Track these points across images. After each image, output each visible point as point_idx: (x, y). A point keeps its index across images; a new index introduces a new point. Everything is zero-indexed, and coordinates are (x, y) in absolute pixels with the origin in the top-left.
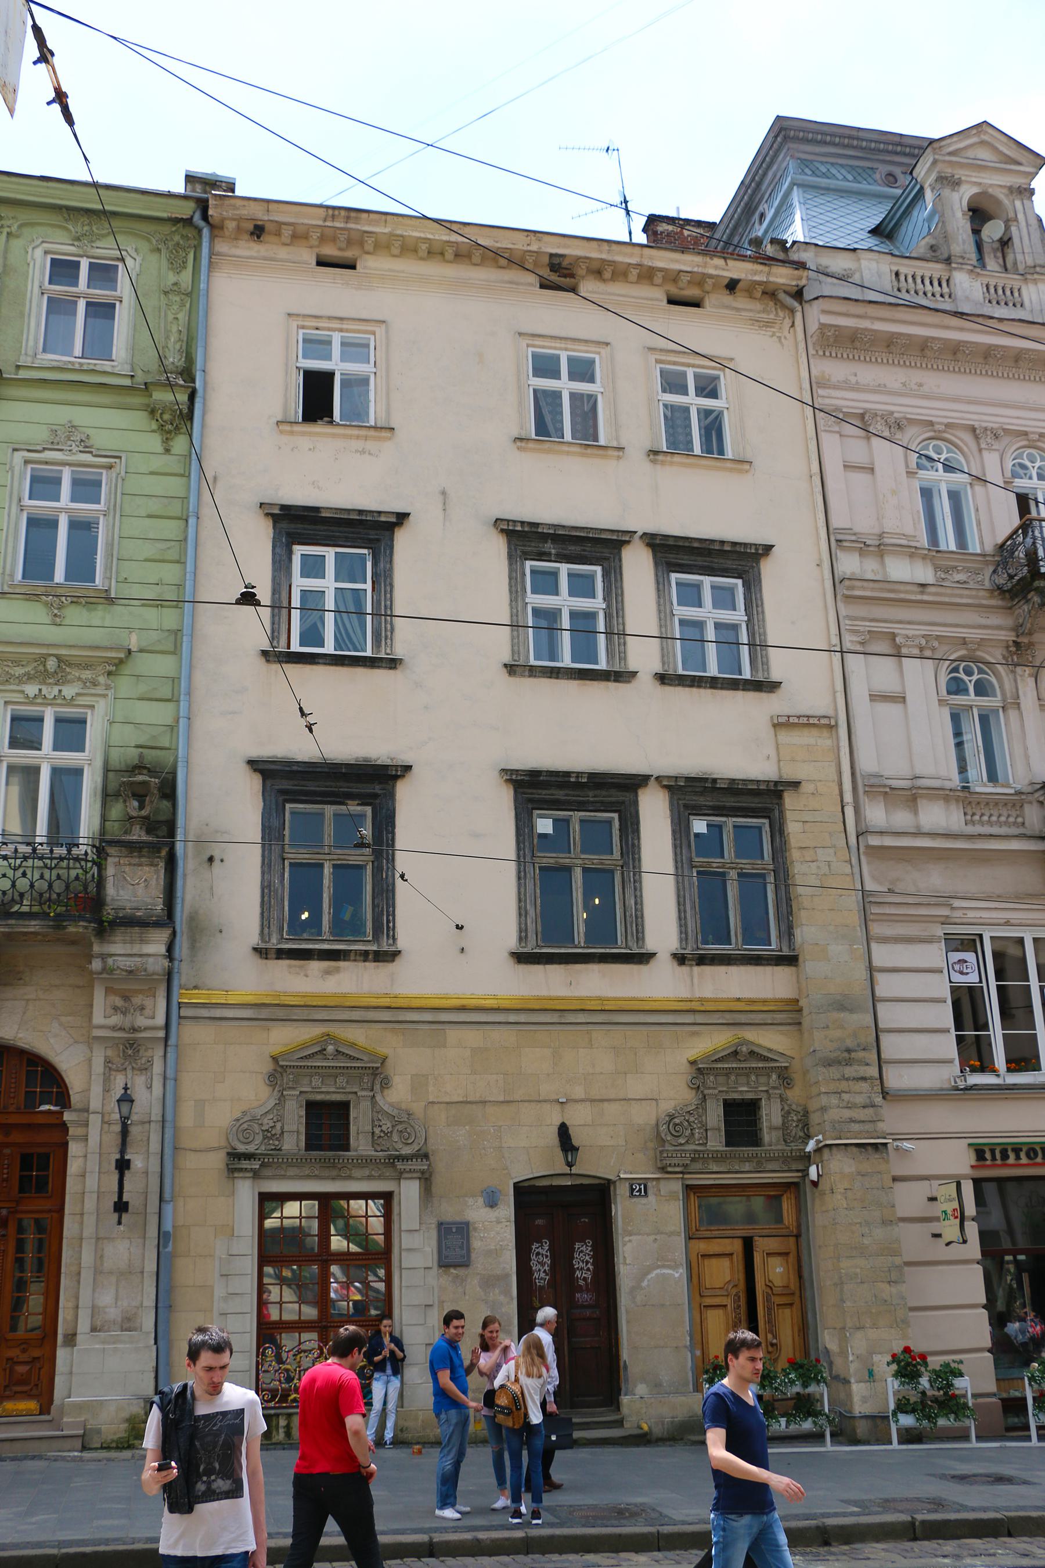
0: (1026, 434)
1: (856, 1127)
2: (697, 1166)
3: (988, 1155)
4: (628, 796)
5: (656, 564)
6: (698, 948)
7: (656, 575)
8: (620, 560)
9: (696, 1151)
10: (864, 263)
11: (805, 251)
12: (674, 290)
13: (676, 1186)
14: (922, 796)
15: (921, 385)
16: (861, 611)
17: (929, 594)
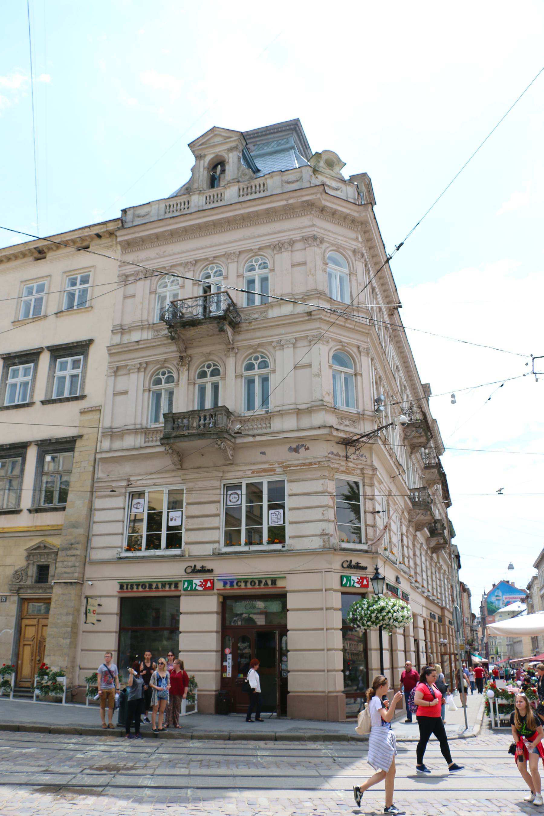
0: (207, 259)
1: (66, 575)
2: (22, 591)
3: (125, 587)
4: (24, 450)
5: (51, 357)
6: (39, 506)
7: (50, 362)
8: (39, 359)
9: (20, 585)
10: (154, 207)
11: (129, 211)
12: (79, 245)
13: (15, 598)
14: (126, 433)
15: (165, 252)
16: (116, 358)
17: (141, 344)
